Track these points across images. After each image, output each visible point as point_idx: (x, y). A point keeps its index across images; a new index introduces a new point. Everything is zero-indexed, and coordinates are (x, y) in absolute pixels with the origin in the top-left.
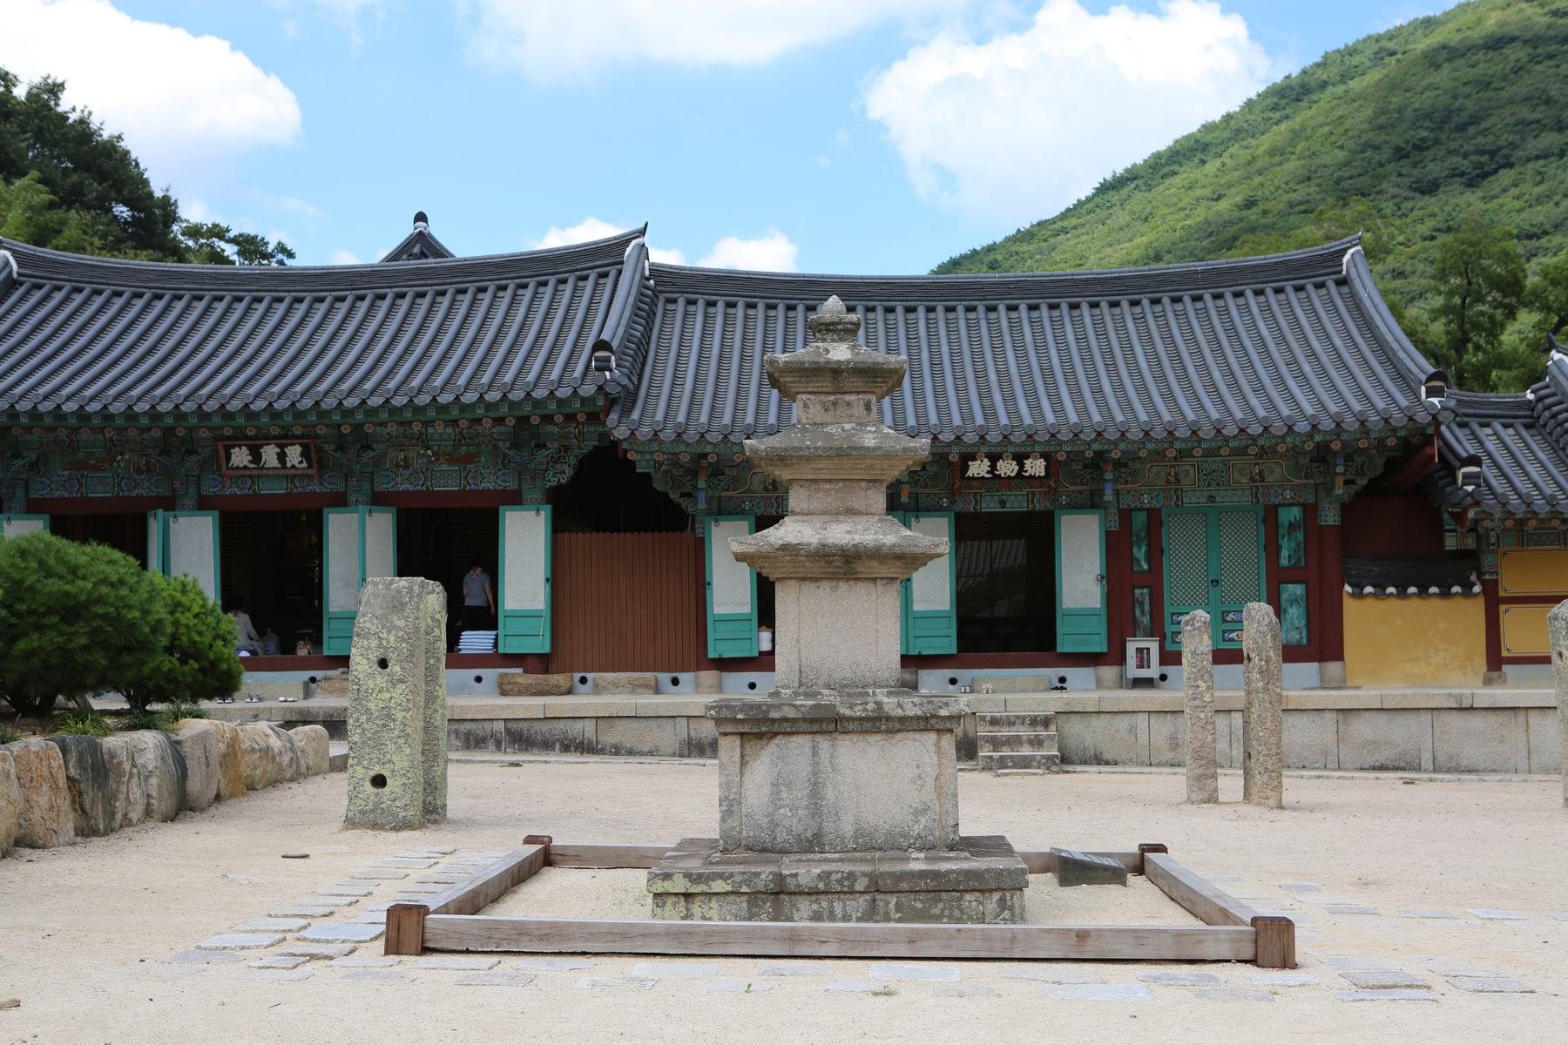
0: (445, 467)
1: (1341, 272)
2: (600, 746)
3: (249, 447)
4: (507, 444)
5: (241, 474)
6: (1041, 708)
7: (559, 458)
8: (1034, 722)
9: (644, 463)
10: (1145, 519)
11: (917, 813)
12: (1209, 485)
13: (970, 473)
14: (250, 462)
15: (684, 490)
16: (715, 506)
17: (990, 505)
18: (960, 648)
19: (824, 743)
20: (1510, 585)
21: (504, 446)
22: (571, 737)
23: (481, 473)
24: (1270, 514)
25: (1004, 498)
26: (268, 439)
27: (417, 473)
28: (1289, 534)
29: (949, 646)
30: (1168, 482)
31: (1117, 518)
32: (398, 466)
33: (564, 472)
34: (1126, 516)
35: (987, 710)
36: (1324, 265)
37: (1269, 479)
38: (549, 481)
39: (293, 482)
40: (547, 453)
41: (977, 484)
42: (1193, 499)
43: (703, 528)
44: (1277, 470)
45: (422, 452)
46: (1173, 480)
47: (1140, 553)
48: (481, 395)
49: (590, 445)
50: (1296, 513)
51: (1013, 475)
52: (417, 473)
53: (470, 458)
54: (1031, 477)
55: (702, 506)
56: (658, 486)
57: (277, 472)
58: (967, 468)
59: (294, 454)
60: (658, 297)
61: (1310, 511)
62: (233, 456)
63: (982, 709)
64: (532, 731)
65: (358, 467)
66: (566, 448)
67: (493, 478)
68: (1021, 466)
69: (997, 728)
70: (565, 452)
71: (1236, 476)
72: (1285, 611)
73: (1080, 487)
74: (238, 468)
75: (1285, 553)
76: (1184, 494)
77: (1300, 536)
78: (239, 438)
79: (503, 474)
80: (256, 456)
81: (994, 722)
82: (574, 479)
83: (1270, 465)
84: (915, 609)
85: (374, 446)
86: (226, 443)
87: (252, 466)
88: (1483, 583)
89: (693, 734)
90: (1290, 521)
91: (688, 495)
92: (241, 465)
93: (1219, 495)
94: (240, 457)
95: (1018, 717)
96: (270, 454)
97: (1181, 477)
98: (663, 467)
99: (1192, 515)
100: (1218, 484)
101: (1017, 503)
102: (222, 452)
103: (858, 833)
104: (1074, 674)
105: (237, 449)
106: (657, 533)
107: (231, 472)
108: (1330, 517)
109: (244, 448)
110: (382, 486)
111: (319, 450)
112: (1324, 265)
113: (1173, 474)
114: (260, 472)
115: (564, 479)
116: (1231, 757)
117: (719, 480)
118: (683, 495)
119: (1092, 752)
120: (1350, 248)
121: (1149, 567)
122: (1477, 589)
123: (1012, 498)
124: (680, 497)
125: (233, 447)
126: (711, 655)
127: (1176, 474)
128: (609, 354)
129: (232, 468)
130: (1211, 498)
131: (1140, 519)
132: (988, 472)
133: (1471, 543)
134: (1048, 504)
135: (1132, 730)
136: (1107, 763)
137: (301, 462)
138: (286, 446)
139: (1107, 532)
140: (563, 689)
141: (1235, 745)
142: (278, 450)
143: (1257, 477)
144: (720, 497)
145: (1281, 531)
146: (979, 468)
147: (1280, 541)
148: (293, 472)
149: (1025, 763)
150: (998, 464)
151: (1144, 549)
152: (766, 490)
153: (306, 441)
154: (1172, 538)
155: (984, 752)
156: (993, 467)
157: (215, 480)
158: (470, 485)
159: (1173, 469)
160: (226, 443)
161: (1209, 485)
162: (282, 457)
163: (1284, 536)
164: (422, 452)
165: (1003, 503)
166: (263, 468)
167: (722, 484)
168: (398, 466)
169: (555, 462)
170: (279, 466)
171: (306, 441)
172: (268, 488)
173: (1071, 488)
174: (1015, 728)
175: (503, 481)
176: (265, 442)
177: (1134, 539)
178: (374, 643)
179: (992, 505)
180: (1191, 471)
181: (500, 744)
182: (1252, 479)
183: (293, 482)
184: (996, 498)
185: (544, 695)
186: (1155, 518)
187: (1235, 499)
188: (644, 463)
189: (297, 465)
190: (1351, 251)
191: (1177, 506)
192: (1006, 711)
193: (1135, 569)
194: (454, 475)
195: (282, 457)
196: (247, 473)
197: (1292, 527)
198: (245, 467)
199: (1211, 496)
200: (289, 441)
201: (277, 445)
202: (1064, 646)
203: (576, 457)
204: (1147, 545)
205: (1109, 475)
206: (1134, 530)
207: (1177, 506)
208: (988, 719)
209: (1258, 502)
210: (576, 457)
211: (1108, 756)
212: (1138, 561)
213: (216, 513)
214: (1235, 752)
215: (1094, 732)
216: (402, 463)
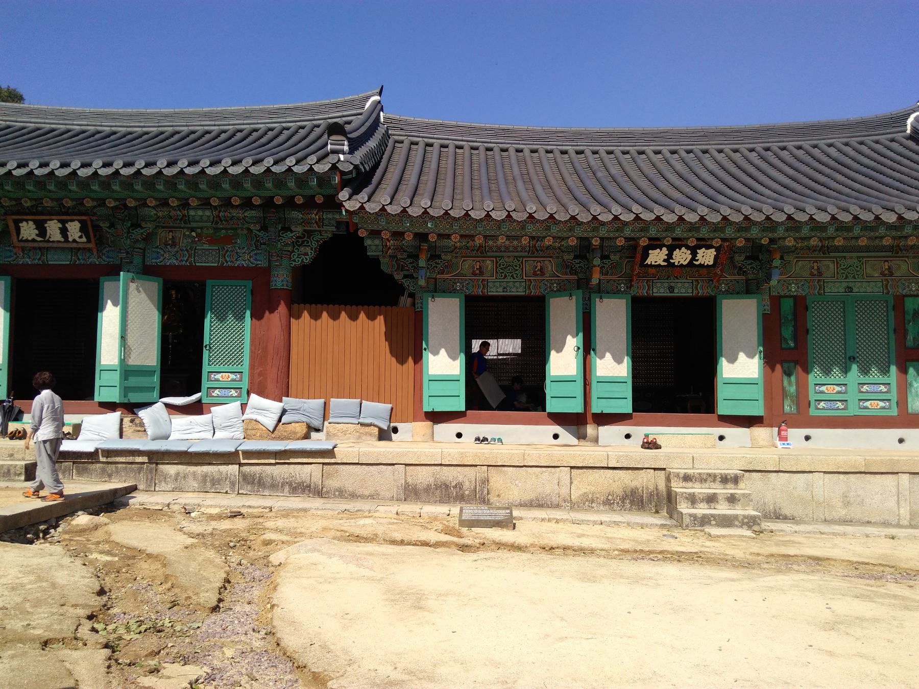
0: (206, 247)
1: (905, 131)
2: (325, 489)
3: (35, 222)
4: (258, 227)
5: (28, 247)
6: (726, 466)
7: (303, 242)
8: (725, 480)
9: (374, 248)
10: (792, 304)
12: (847, 277)
13: (648, 261)
14: (37, 235)
15: (406, 273)
16: (432, 287)
17: (660, 290)
18: (635, 410)
21: (255, 228)
22: (299, 480)
23: (237, 253)
25: (673, 284)
26: (51, 213)
27: (182, 250)
28: (914, 321)
29: (626, 406)
30: (812, 275)
31: (769, 303)
32: (166, 244)
33: (306, 254)
34: (776, 301)
35: (676, 466)
36: (893, 125)
37: (897, 274)
38: (294, 261)
39: (76, 255)
40: (291, 235)
41: (653, 271)
42: (835, 288)
43: (422, 303)
44: (904, 267)
45: (187, 233)
46: (816, 272)
47: (787, 332)
48: (225, 168)
49: (329, 231)
51: (685, 263)
52: (182, 250)
53: (228, 240)
54: (701, 266)
55: (422, 282)
56: (386, 266)
57: (60, 245)
58: (647, 255)
59: (74, 229)
60: (389, 138)
62: (22, 229)
63: (672, 465)
64: (263, 475)
65: (128, 241)
66: (309, 233)
67: (247, 257)
68: (694, 254)
69: (690, 484)
70: (309, 237)
71: (869, 271)
72: (911, 385)
73: (737, 277)
74: (27, 241)
75: (910, 337)
76: (825, 284)
78: (20, 213)
79: (256, 254)
80: (42, 231)
81: (687, 478)
82: (315, 260)
83: (897, 262)
84: (598, 374)
85: (143, 224)
86: (15, 217)
87: (39, 239)
89: (410, 480)
90: (914, 310)
91: (410, 277)
92: (30, 238)
93: (855, 286)
94: (28, 230)
95: (709, 475)
96: (53, 228)
97: (823, 269)
98: (390, 251)
99: (832, 302)
100: (854, 277)
101: (684, 289)
102: (12, 225)
105: (24, 224)
106: (383, 307)
107: (22, 244)
109: (31, 223)
110: (151, 261)
111: (97, 228)
112: (893, 125)
113: (816, 268)
114: (46, 245)
115: (307, 260)
116: (899, 515)
117: (436, 263)
118: (405, 277)
119: (772, 507)
120: (912, 113)
121: (796, 348)
123: (679, 285)
124: (403, 278)
125: (21, 221)
126: (427, 408)
127: (818, 269)
128: (343, 138)
129: (22, 241)
130: (850, 289)
131: (787, 306)
132: (664, 260)
134: (709, 291)
136: (786, 518)
137: (81, 237)
138: (67, 221)
139: (764, 314)
140: (299, 435)
141: (902, 503)
142: (61, 226)
143: (886, 272)
144: (436, 279)
145: (908, 317)
146: (657, 257)
147: (906, 325)
148: (75, 245)
149: (726, 521)
150: (675, 253)
151: (791, 329)
152: (474, 274)
153: (83, 218)
154: (813, 319)
155: (684, 508)
156: (670, 256)
157: (10, 251)
158: (227, 262)
159: (815, 264)
160: (15, 217)
161: (847, 277)
162: (64, 231)
163: (909, 322)
164: (187, 233)
165: (671, 289)
166: (48, 241)
167: (439, 266)
168: (166, 244)
169: (299, 246)
170: (62, 240)
171: (83, 218)
172: (54, 259)
173: (730, 278)
174: (707, 486)
175: (256, 260)
176: (48, 217)
177: (783, 321)
179: (662, 290)
180: (831, 266)
181: (234, 486)
182: (883, 274)
183: (76, 255)
184: (666, 285)
185: (282, 439)
186: (800, 305)
187: (868, 289)
188: (374, 248)
189: (78, 240)
191: (819, 294)
192: (693, 468)
193: (784, 346)
194: (214, 253)
195: (64, 231)
196: (36, 245)
198: (34, 240)
199: (848, 287)
200: (69, 218)
201: (59, 221)
202: (723, 408)
203: (317, 241)
204: (793, 327)
205: (777, 263)
206: (782, 313)
207: (819, 294)
208: (682, 476)
209: (888, 293)
210: (317, 241)
211: (786, 511)
212: (786, 340)
213: (9, 278)
214: (902, 511)
215: (774, 489)
216: (170, 242)
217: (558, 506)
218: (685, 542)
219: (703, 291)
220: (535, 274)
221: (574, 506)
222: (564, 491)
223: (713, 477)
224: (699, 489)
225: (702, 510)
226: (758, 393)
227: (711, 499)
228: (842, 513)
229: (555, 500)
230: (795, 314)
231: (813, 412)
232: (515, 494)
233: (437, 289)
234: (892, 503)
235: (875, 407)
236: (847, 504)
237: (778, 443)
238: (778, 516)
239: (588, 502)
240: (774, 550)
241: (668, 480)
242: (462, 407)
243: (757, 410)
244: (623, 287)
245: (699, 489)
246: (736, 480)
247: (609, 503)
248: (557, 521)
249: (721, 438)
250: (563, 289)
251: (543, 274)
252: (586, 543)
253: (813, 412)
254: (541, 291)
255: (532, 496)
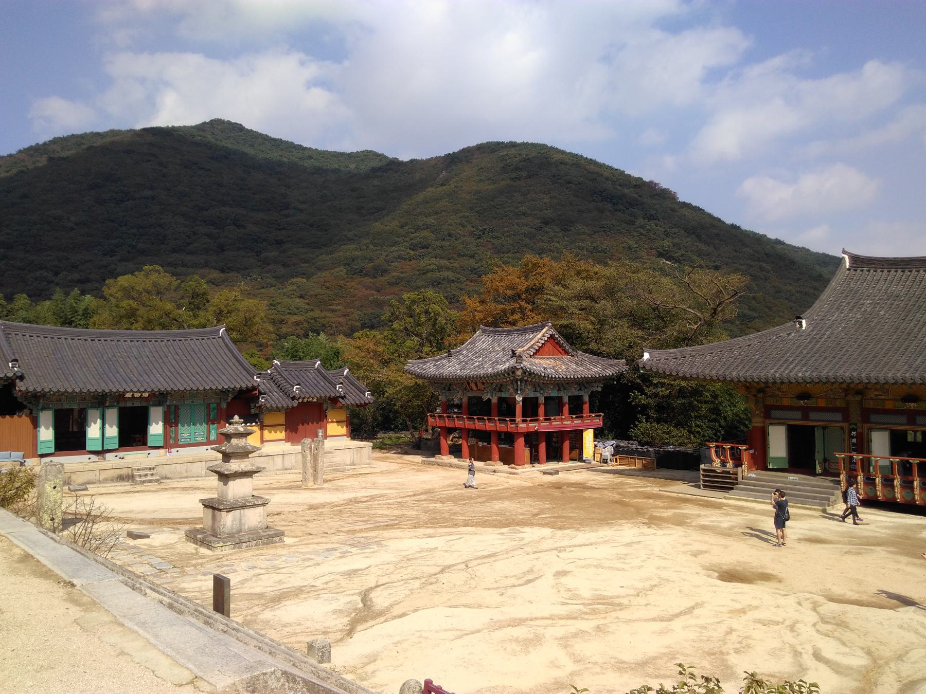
8: (150, 469)
11: (259, 522)
17: (129, 405)
18: (120, 446)
19: (242, 511)
20: (266, 422)
24: (209, 405)
34: (169, 407)
47: (172, 417)
50: (215, 405)
61: (218, 405)
75: (211, 416)
77: (216, 411)
81: (138, 470)
88: (260, 422)
101: (137, 404)
103: (248, 528)
104: (152, 452)
108: (224, 406)
118: (28, 403)
122: (259, 424)
126: (39, 453)
130: (193, 402)
131: (173, 408)
133: (257, 412)
135: (175, 468)
146: (129, 395)
149: (150, 481)
155: (138, 479)
165: (133, 404)
178: (53, 483)
186: (177, 408)
190: (222, 330)
197: (214, 409)
211: (169, 476)
217: (95, 483)
218: (138, 488)
219: (144, 404)
220: (82, 400)
221: (100, 482)
222: (97, 478)
223: (146, 468)
224: (142, 473)
225: (143, 479)
226: (162, 438)
227: (146, 475)
228: (185, 475)
229: (94, 481)
230: (175, 411)
231: (179, 443)
232: (80, 480)
233: (45, 408)
234: (200, 471)
235: (199, 439)
236: (187, 472)
237: (168, 454)
238: (166, 478)
239: (105, 480)
240: (163, 487)
241: (132, 470)
242: (53, 451)
243: (162, 444)
244: (115, 404)
245: (142, 473)
246: (153, 469)
247: (112, 480)
248: (98, 487)
249: (149, 454)
250: (93, 407)
251: (85, 400)
252: (111, 492)
253: (179, 443)
254: (85, 406)
255: (86, 481)
